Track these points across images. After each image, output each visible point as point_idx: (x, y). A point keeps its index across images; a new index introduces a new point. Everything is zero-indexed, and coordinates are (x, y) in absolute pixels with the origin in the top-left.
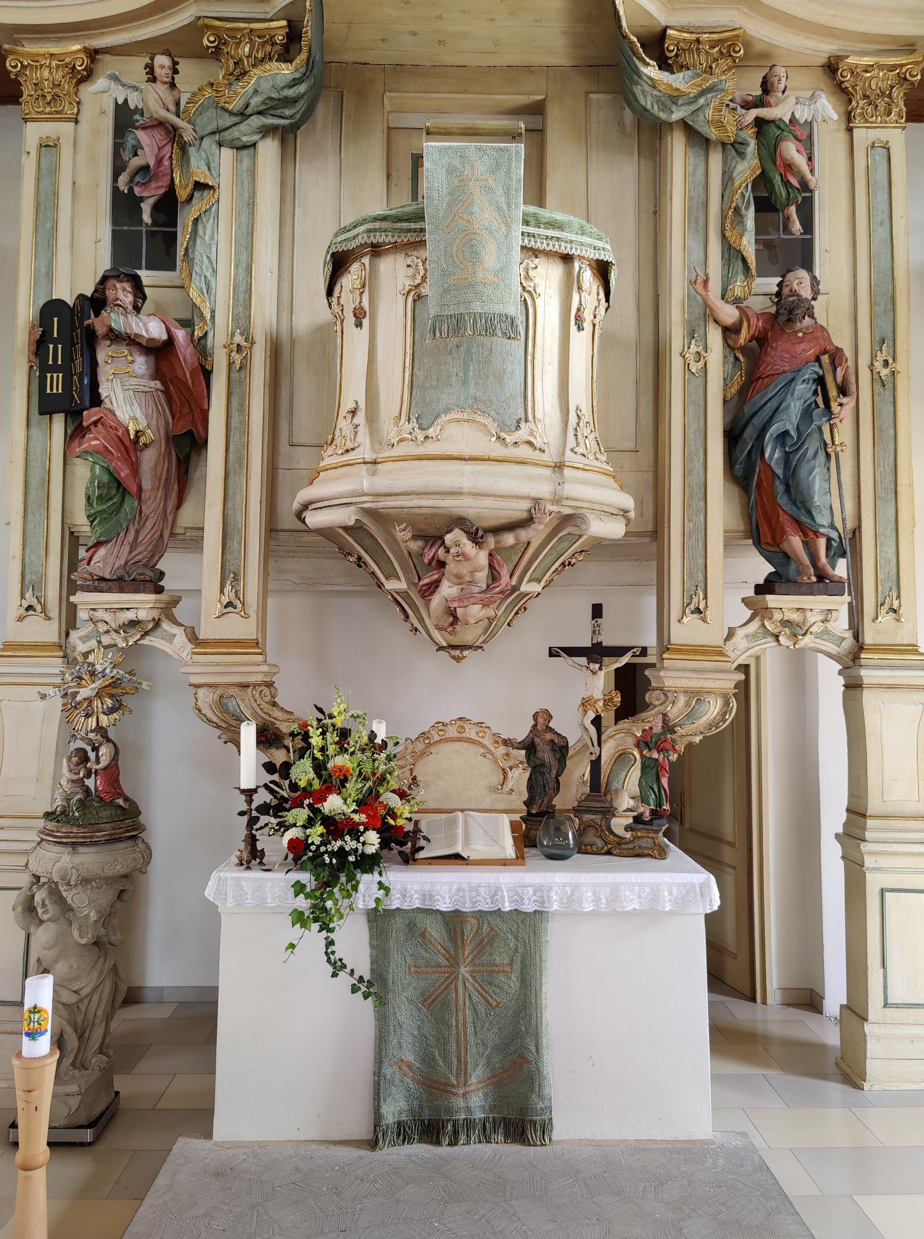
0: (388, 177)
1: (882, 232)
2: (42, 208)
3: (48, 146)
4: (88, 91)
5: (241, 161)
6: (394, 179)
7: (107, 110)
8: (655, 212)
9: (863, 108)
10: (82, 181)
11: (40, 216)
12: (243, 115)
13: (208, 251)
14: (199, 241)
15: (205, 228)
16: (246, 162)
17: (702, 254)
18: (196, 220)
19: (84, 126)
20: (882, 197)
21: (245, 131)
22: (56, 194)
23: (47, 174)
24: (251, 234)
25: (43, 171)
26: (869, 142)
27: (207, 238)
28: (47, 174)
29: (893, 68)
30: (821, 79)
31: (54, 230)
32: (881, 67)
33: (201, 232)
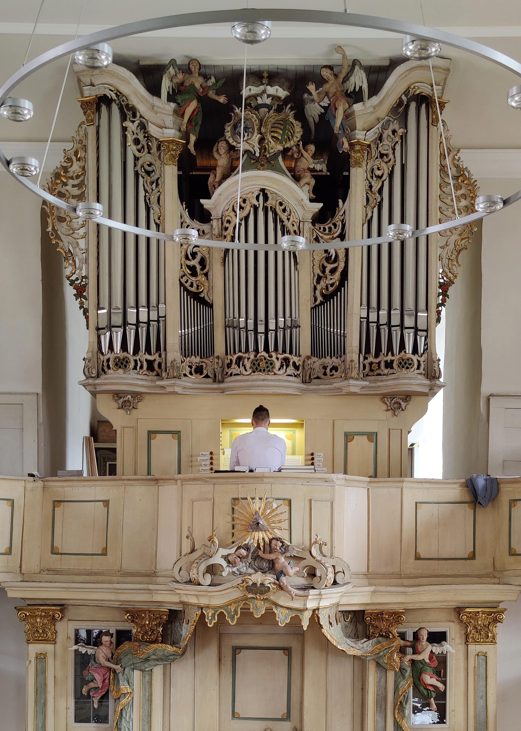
0: (220, 660)
1: (482, 702)
2: (39, 692)
3: (41, 658)
4: (60, 626)
5: (144, 677)
6: (223, 661)
7: (71, 636)
8: (362, 689)
9: (473, 634)
10: (59, 674)
11: (38, 696)
12: (147, 660)
13: (128, 725)
14: (123, 720)
15: (126, 712)
16: (147, 677)
17: (383, 724)
18: (122, 710)
19: (58, 646)
20: (482, 683)
21: (147, 666)
22: (45, 685)
23: (41, 672)
24: (150, 716)
25: (39, 672)
26: (477, 652)
27: (127, 718)
28: (41, 672)
29: (490, 614)
30: (453, 616)
31: (45, 704)
32: (483, 613)
33: (124, 715)
